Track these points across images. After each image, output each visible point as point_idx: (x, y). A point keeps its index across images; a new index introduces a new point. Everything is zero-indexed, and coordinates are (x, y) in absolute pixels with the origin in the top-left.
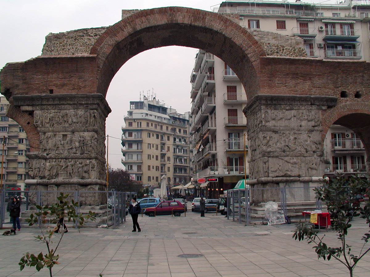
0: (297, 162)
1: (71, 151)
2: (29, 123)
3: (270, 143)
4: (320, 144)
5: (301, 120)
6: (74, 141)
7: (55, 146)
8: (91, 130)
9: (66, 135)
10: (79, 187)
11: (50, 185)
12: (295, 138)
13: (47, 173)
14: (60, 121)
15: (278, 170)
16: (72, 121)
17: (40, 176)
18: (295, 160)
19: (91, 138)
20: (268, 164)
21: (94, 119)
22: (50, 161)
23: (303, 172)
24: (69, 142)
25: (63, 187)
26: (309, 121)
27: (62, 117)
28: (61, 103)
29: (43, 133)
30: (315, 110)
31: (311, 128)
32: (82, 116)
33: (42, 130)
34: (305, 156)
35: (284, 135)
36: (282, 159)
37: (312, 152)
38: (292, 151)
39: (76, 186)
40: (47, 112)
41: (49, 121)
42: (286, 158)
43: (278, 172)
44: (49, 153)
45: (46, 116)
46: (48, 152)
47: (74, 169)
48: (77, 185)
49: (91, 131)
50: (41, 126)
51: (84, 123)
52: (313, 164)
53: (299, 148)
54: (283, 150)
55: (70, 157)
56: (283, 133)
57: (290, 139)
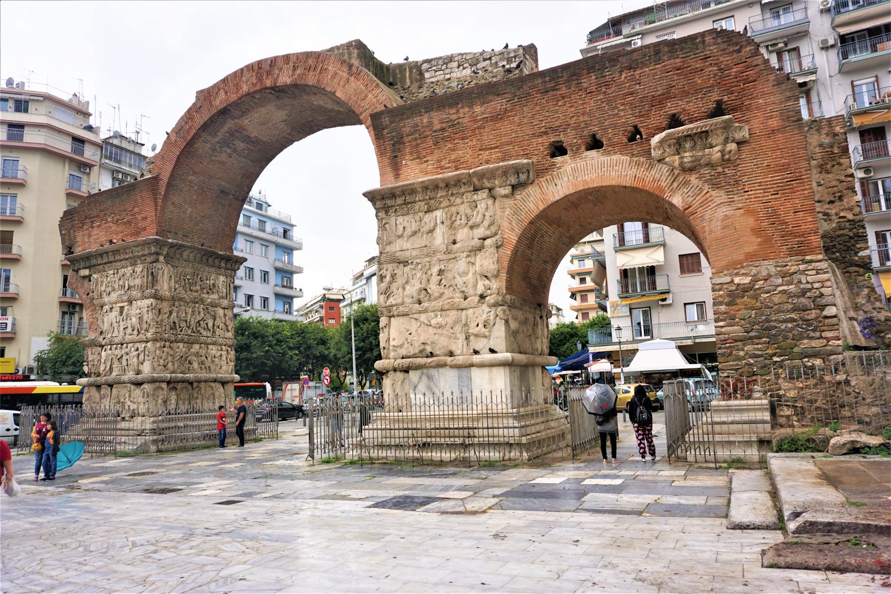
0: (444, 323)
3: (394, 287)
4: (496, 276)
5: (455, 229)
9: (123, 307)
10: (133, 387)
12: (441, 272)
13: (102, 368)
15: (406, 342)
18: (439, 319)
20: (389, 332)
23: (458, 346)
25: (116, 387)
26: (472, 228)
28: (117, 257)
30: (484, 201)
31: (476, 242)
34: (463, 307)
35: (420, 266)
36: (416, 319)
37: (478, 298)
38: (436, 299)
39: (129, 385)
42: (423, 317)
43: (406, 345)
52: (478, 325)
53: (448, 293)
54: (415, 299)
56: (418, 264)
57: (432, 275)
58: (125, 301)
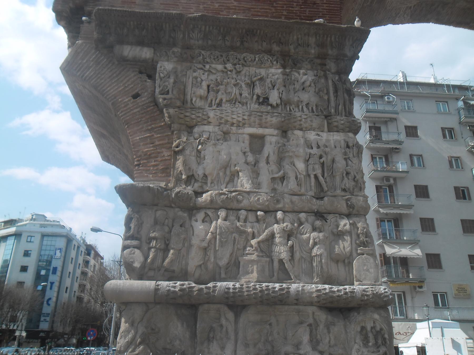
1: (279, 187)
2: (136, 96)
6: (291, 157)
7: (226, 168)
8: (341, 127)
9: (262, 138)
11: (206, 306)
14: (241, 95)
16: (281, 99)
17: (166, 270)
19: (343, 151)
21: (346, 95)
22: (207, 215)
24: (273, 158)
27: (247, 84)
29: (184, 127)
32: (310, 86)
33: (182, 116)
39: (310, 310)
40: (202, 69)
41: (206, 93)
44: (200, 190)
45: (196, 78)
46: (201, 187)
47: (296, 248)
48: (314, 308)
49: (343, 131)
50: (178, 103)
51: (317, 106)
55: (280, 206)
58: (271, 126)
